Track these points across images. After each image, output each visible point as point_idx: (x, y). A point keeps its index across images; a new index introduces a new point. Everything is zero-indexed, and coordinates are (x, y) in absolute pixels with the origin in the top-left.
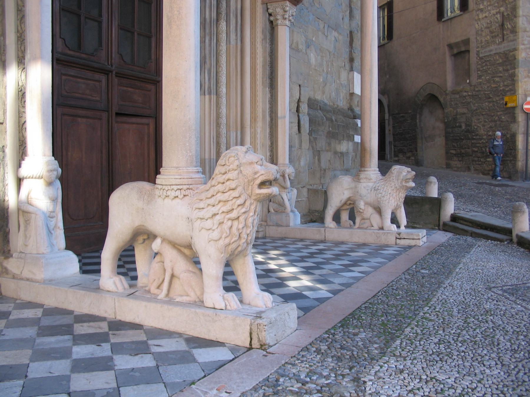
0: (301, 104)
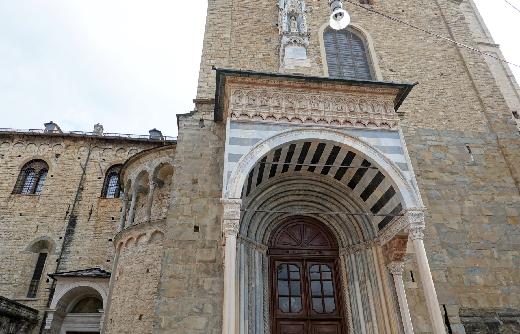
0: (449, 318)
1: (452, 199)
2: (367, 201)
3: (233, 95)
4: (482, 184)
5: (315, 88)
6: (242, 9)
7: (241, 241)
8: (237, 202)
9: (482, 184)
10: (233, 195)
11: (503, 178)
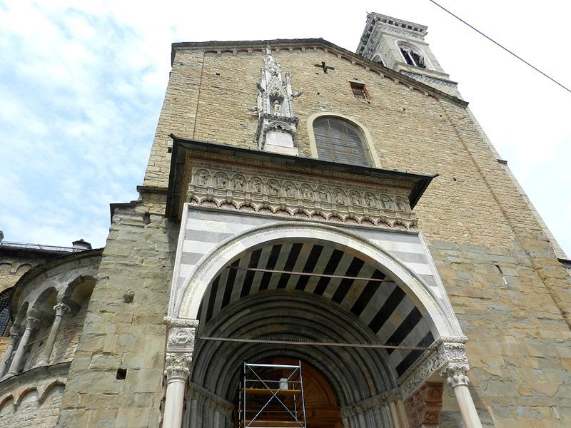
1: (489, 333)
2: (379, 333)
3: (195, 175)
4: (522, 313)
5: (307, 174)
6: (212, 88)
7: (194, 395)
8: (191, 324)
9: (522, 313)
10: (184, 313)
11: (545, 307)
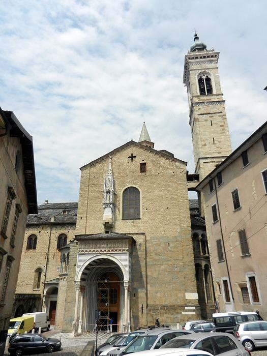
4: (170, 259)
